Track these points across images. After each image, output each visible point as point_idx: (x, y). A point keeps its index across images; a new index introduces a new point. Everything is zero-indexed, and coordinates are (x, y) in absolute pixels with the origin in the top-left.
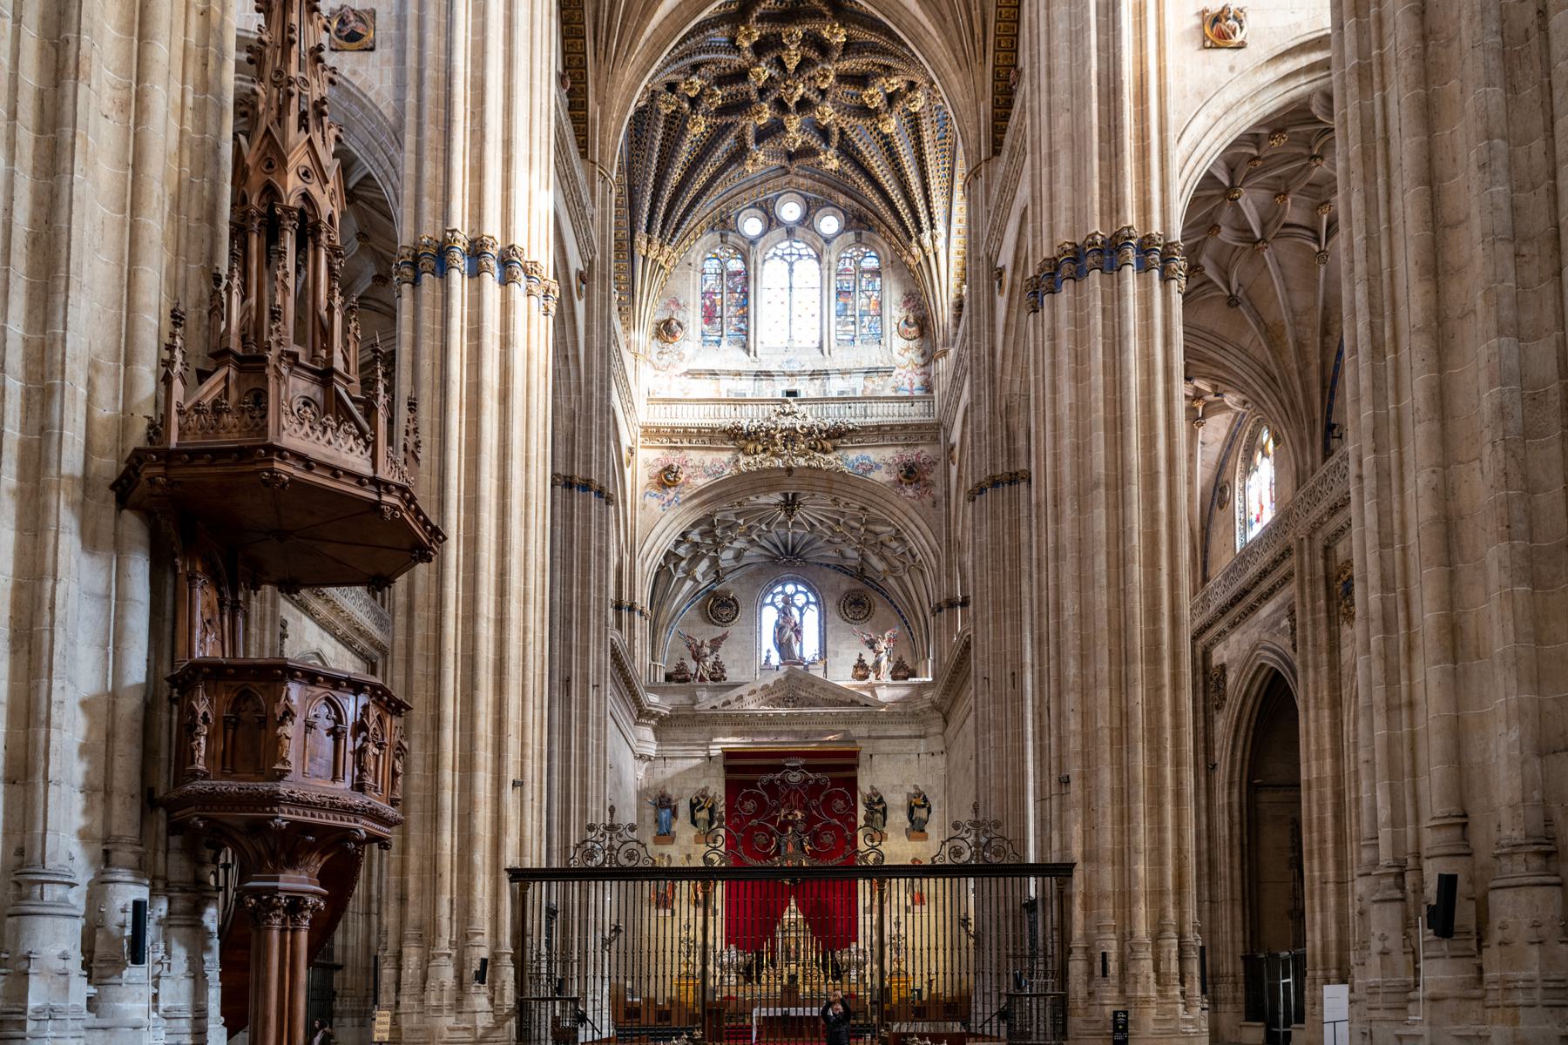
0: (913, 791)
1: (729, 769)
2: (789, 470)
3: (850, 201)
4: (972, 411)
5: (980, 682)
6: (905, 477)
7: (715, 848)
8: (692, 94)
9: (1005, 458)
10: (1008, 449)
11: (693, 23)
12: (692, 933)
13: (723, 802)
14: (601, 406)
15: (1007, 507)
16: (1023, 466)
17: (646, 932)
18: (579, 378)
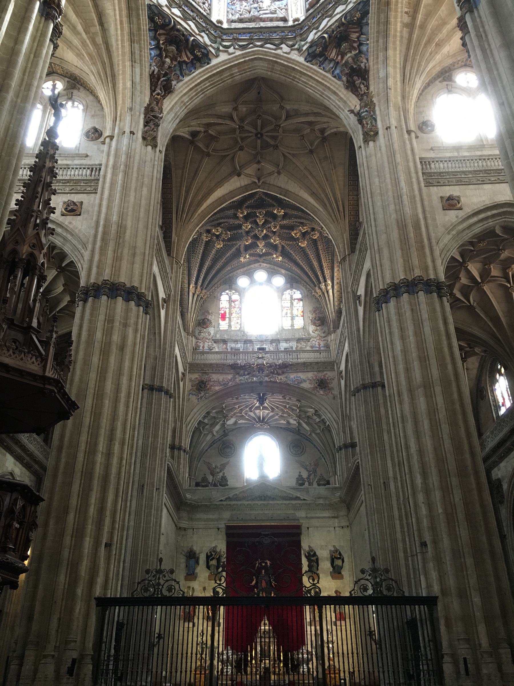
0: (333, 549)
1: (228, 535)
2: (261, 383)
3: (287, 272)
4: (350, 355)
5: (366, 487)
6: (318, 385)
7: (220, 585)
8: (218, 233)
9: (369, 376)
10: (370, 372)
11: (219, 209)
12: (204, 638)
13: (225, 556)
14: (170, 354)
15: (372, 398)
16: (378, 379)
17: (176, 637)
18: (160, 342)
